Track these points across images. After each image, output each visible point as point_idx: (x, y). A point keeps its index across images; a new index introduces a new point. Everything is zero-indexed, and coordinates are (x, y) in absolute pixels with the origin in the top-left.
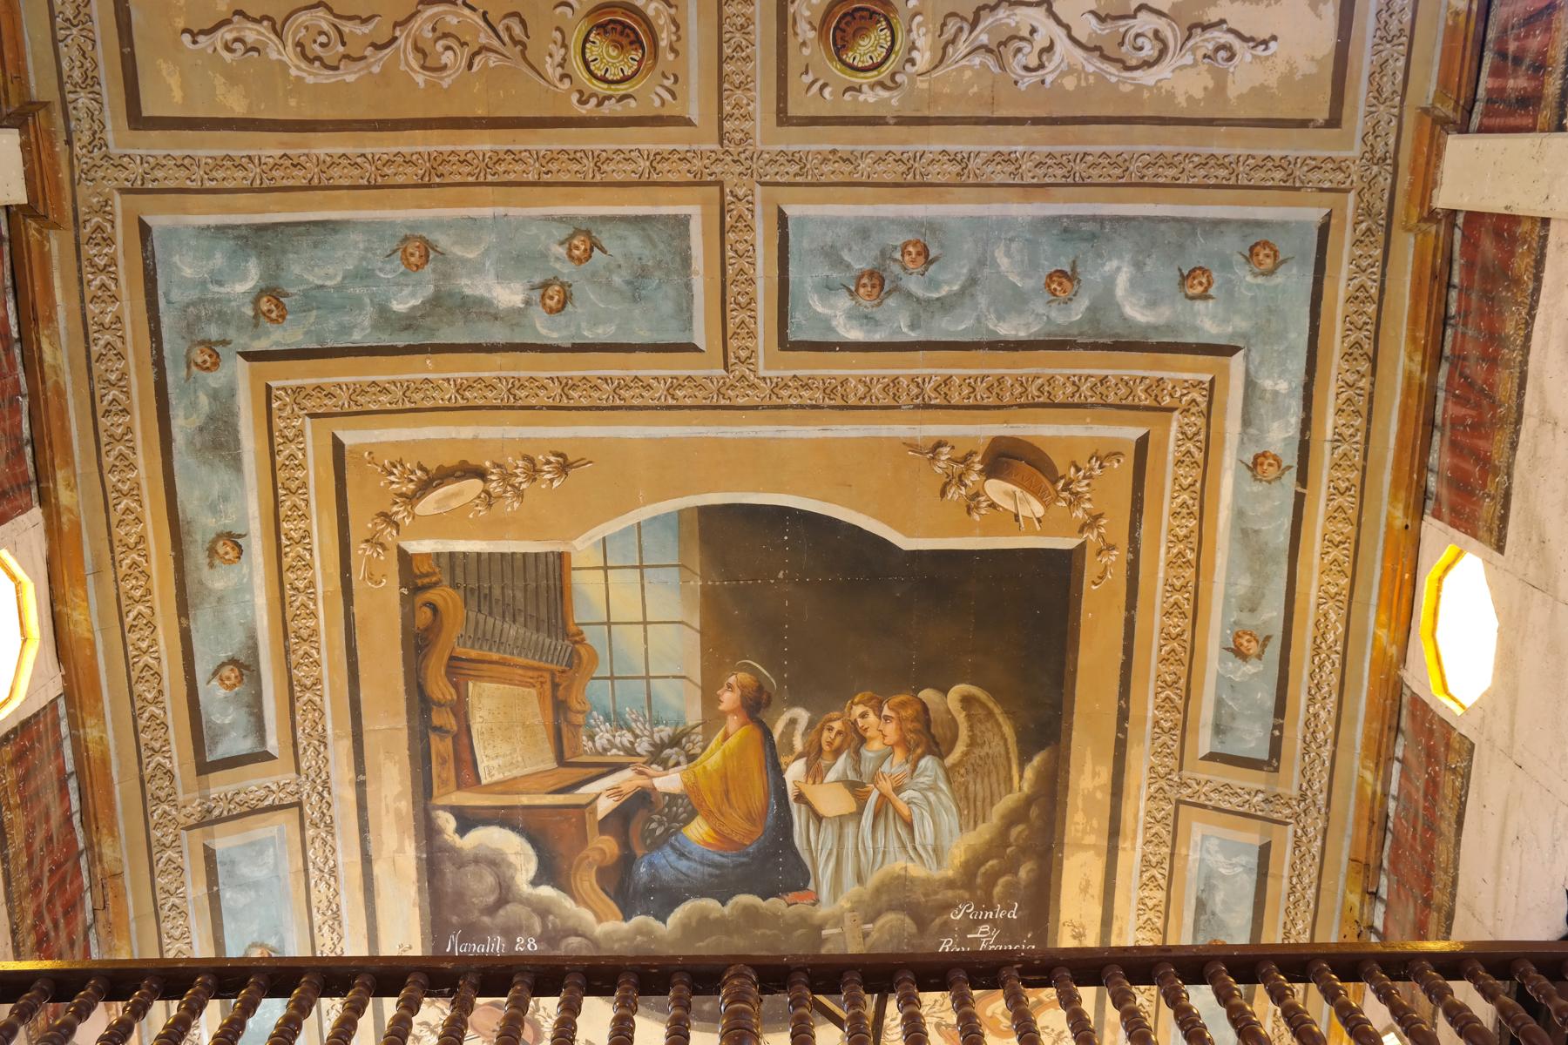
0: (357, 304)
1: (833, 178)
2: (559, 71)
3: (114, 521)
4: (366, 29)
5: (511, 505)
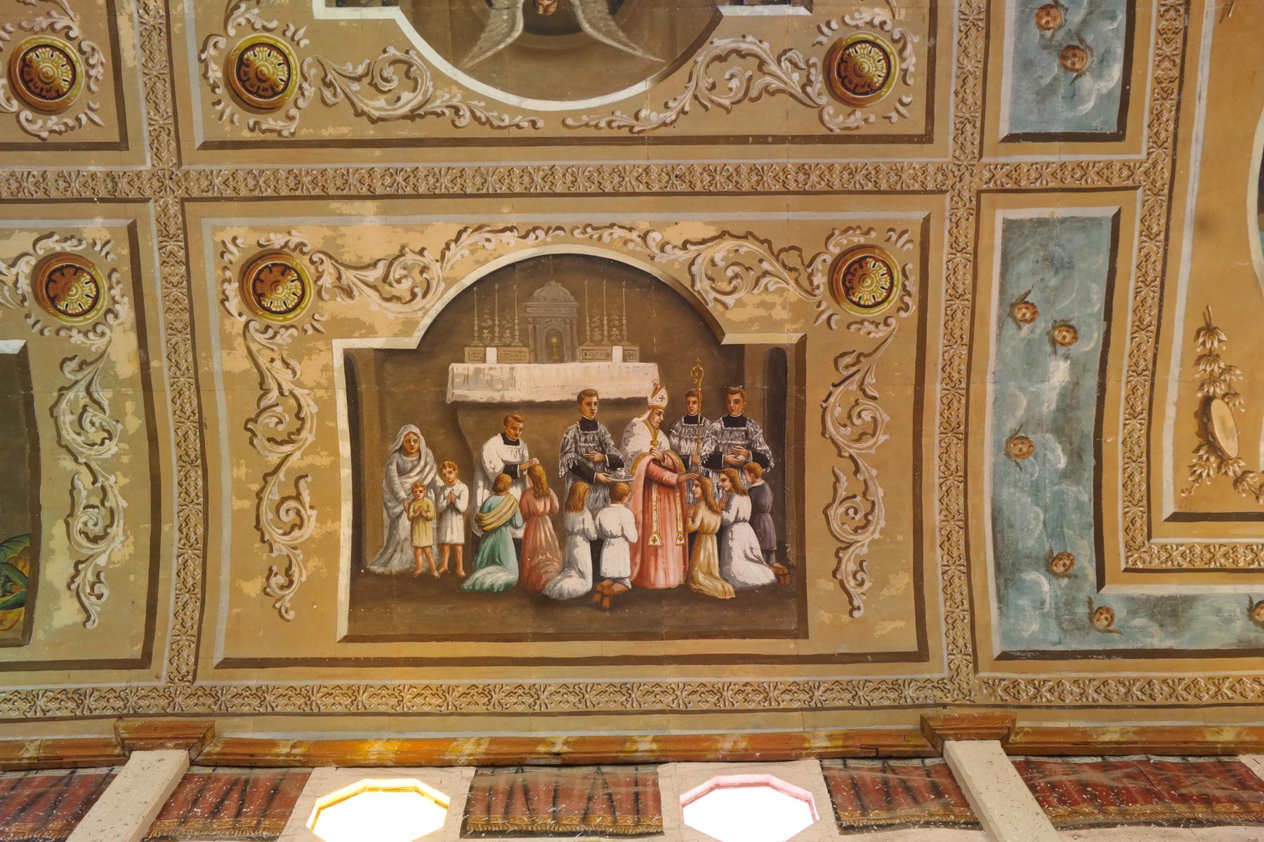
0: (1059, 496)
1: (979, 93)
2: (881, 327)
3: (1242, 700)
4: (843, 478)
5: (1238, 377)
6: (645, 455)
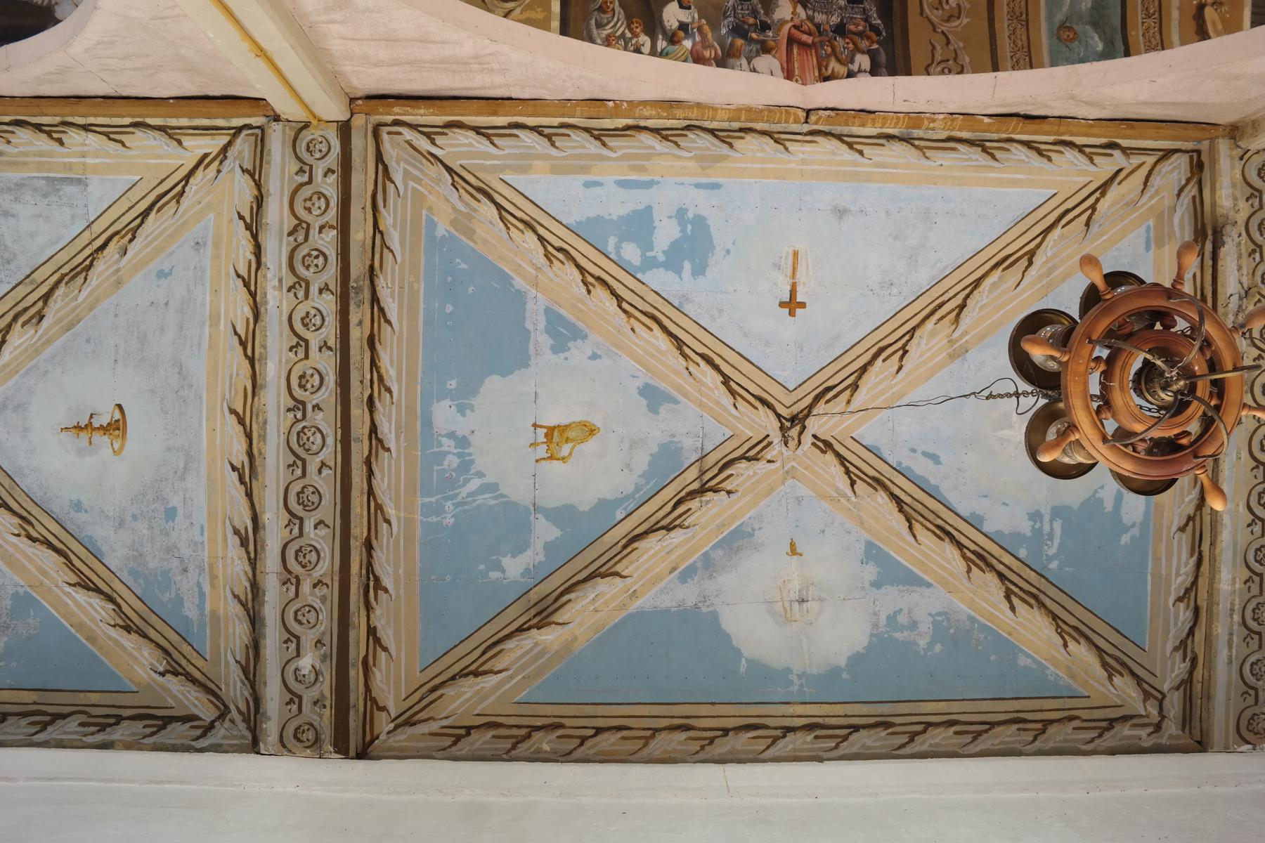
4: (938, 48)
6: (787, 22)
